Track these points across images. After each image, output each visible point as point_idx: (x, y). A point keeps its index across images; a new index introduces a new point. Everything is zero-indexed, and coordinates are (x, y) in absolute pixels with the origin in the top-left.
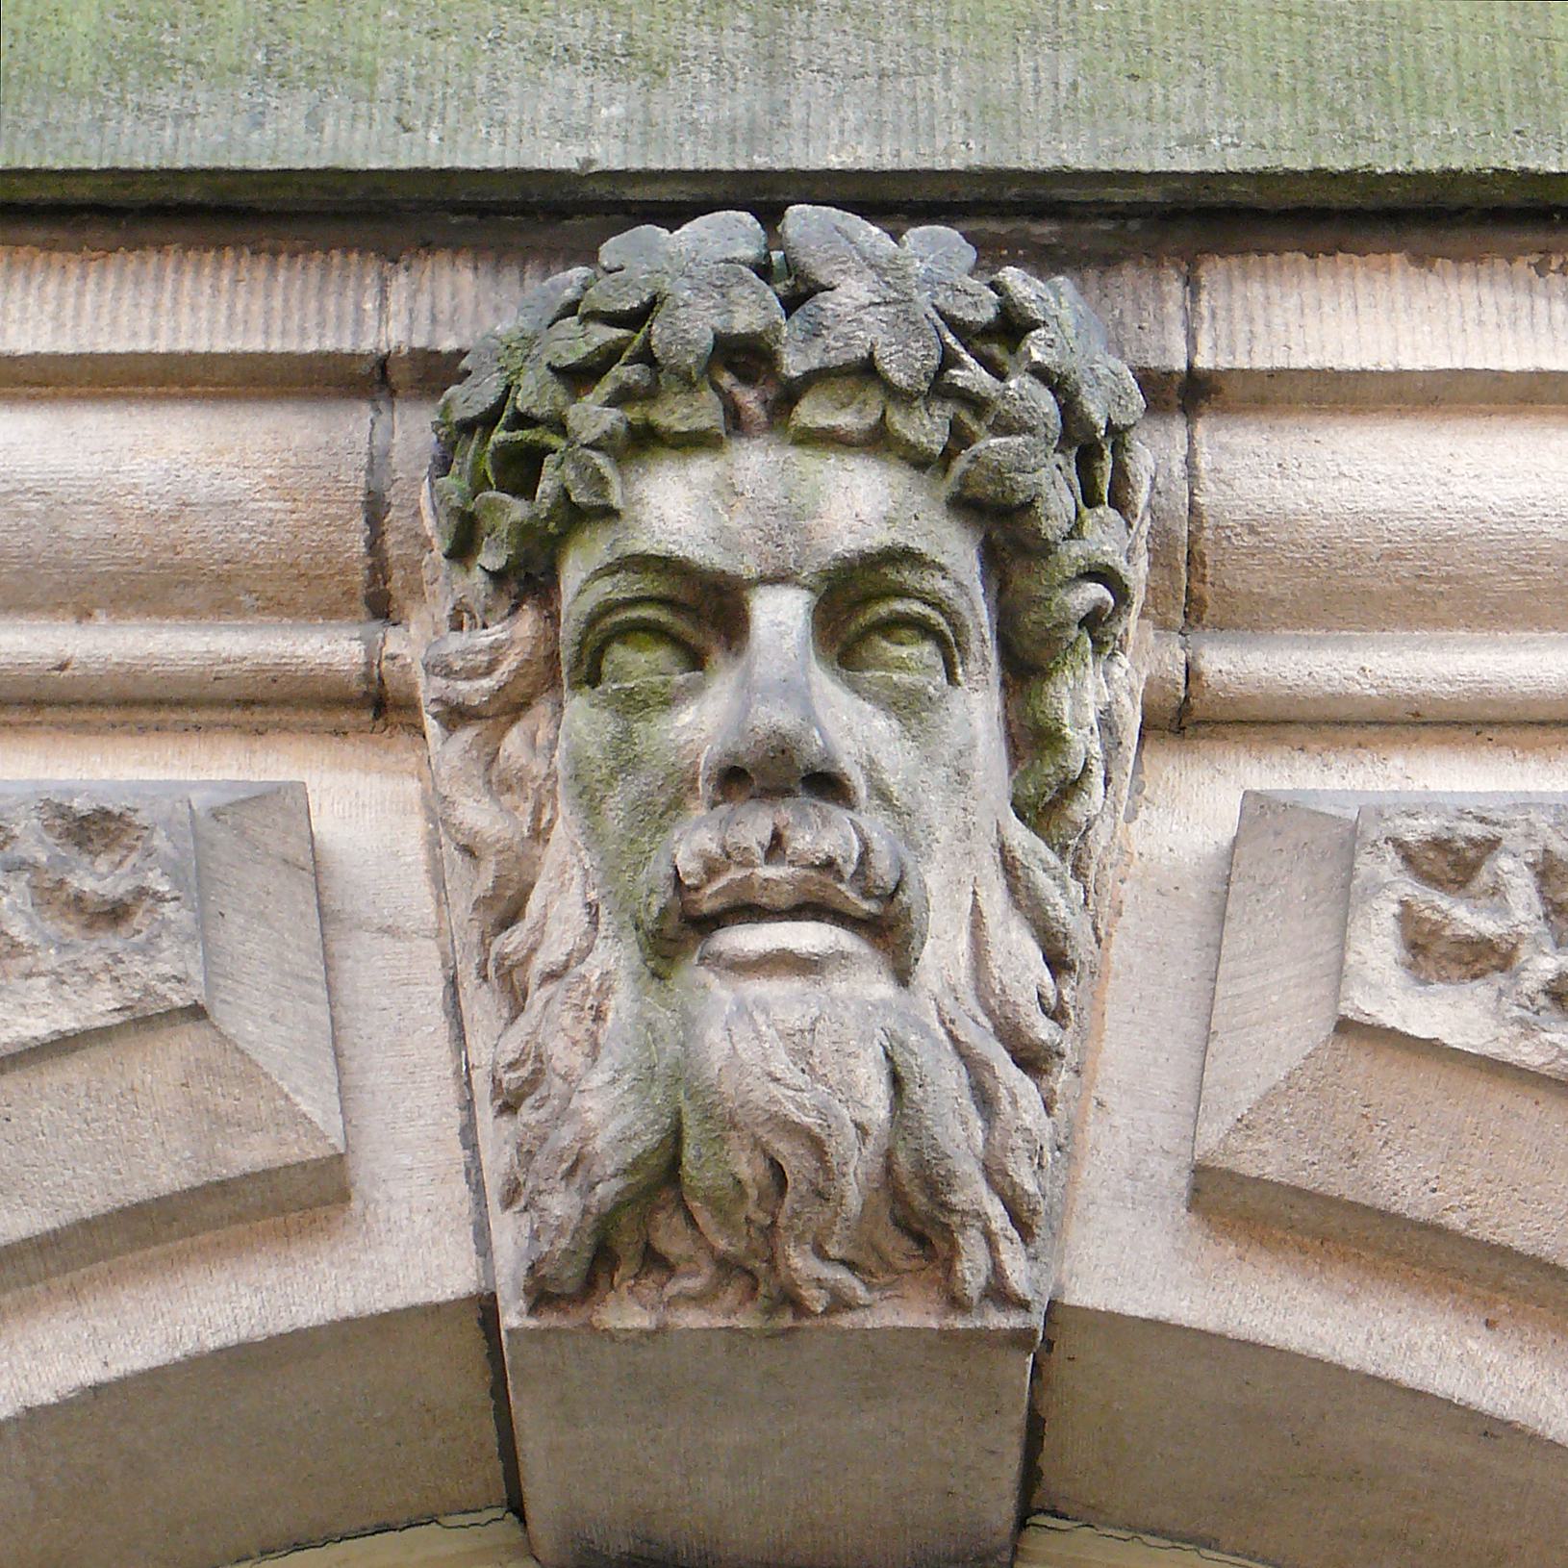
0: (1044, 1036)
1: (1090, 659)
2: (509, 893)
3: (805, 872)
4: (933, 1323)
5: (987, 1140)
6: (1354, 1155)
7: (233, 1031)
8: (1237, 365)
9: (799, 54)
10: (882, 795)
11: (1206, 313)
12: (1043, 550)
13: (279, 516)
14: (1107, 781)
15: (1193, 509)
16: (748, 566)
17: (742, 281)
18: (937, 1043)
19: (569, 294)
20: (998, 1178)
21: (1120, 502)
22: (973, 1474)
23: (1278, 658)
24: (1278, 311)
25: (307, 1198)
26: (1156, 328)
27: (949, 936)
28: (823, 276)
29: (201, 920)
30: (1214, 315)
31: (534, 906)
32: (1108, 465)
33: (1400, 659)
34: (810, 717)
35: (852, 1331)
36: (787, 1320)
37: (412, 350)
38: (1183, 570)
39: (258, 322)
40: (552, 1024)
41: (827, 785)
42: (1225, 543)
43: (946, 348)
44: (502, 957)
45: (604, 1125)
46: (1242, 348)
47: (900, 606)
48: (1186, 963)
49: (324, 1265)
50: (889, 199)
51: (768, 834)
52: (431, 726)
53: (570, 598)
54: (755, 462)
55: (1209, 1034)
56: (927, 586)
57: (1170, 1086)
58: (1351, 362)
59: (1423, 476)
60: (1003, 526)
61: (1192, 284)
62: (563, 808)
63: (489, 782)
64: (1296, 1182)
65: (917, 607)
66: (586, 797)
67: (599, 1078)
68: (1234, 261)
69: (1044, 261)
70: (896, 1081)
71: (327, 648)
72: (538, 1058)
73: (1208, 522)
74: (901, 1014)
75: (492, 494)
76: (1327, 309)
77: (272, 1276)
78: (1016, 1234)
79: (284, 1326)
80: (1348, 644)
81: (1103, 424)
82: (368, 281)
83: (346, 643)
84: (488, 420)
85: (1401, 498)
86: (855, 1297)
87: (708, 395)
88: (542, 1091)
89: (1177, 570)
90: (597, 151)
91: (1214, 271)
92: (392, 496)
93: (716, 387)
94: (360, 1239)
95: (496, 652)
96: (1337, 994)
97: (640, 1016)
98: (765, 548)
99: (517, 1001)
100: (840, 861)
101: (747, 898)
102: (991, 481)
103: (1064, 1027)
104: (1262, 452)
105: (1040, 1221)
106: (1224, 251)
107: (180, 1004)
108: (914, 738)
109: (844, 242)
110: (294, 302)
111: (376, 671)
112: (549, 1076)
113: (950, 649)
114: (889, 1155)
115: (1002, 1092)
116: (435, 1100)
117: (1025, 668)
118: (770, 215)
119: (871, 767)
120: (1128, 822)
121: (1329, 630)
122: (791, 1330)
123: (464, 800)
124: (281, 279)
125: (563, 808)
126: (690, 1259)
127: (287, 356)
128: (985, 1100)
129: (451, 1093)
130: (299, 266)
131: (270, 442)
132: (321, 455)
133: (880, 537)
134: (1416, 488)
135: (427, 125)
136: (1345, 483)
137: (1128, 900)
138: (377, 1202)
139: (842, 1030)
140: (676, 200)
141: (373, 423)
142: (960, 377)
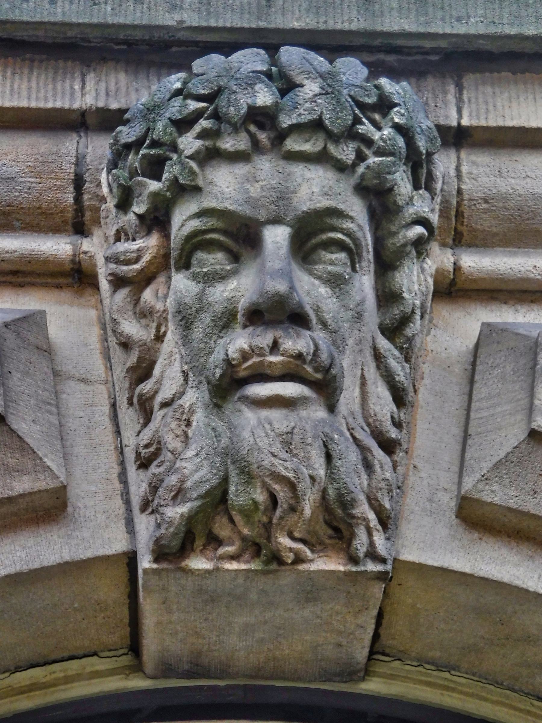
0: (394, 436)
1: (415, 260)
2: (144, 365)
3: (288, 359)
4: (342, 568)
5: (369, 484)
6: (535, 493)
10: (324, 324)
11: (466, 100)
12: (398, 210)
13: (34, 185)
14: (422, 317)
15: (459, 192)
16: (262, 216)
18: (347, 439)
19: (178, 85)
21: (429, 188)
22: (352, 636)
24: (499, 100)
26: (443, 106)
28: (299, 79)
30: (469, 101)
31: (157, 371)
32: (425, 171)
34: (292, 288)
35: (304, 571)
36: (274, 566)
38: (454, 219)
39: (24, 93)
41: (298, 319)
42: (473, 207)
43: (355, 115)
44: (141, 396)
45: (191, 475)
46: (483, 117)
47: (332, 235)
48: (453, 402)
49: (55, 537)
50: (330, 44)
51: (271, 341)
52: (104, 284)
53: (177, 228)
54: (266, 166)
55: (466, 436)
56: (344, 226)
57: (447, 459)
60: (379, 199)
61: (460, 88)
62: (171, 326)
63: (135, 313)
64: (510, 505)
65: (340, 236)
66: (184, 321)
67: (190, 453)
68: (478, 75)
69: (395, 74)
70: (329, 457)
71: (54, 248)
72: (159, 443)
73: (466, 197)
74: (331, 425)
75: (140, 178)
76: (522, 99)
77: (31, 542)
79: (36, 565)
80: (528, 255)
81: (424, 152)
82: (76, 75)
83: (63, 245)
84: (138, 144)
86: (307, 556)
87: (244, 135)
89: (451, 219)
90: (185, 16)
91: (469, 80)
92: (87, 177)
93: (248, 132)
94: (72, 524)
95: (140, 253)
98: (270, 207)
99: (147, 416)
100: (305, 354)
101: (261, 371)
102: (375, 178)
103: (401, 431)
104: (491, 165)
105: (391, 522)
106: (475, 71)
109: (308, 65)
110: (41, 84)
112: (164, 451)
113: (354, 254)
114: (324, 491)
115: (376, 462)
116: (106, 461)
117: (386, 265)
118: (272, 49)
119: (317, 310)
120: (427, 336)
121: (519, 248)
122: (276, 571)
123: (124, 321)
124: (35, 73)
125: (171, 326)
126: (230, 538)
127: (39, 109)
128: (368, 466)
129: (113, 457)
130: (43, 68)
131: (30, 151)
132: (54, 157)
136: (529, 180)
137: (427, 371)
138: (79, 508)
139: (305, 433)
140: (228, 43)
142: (361, 129)
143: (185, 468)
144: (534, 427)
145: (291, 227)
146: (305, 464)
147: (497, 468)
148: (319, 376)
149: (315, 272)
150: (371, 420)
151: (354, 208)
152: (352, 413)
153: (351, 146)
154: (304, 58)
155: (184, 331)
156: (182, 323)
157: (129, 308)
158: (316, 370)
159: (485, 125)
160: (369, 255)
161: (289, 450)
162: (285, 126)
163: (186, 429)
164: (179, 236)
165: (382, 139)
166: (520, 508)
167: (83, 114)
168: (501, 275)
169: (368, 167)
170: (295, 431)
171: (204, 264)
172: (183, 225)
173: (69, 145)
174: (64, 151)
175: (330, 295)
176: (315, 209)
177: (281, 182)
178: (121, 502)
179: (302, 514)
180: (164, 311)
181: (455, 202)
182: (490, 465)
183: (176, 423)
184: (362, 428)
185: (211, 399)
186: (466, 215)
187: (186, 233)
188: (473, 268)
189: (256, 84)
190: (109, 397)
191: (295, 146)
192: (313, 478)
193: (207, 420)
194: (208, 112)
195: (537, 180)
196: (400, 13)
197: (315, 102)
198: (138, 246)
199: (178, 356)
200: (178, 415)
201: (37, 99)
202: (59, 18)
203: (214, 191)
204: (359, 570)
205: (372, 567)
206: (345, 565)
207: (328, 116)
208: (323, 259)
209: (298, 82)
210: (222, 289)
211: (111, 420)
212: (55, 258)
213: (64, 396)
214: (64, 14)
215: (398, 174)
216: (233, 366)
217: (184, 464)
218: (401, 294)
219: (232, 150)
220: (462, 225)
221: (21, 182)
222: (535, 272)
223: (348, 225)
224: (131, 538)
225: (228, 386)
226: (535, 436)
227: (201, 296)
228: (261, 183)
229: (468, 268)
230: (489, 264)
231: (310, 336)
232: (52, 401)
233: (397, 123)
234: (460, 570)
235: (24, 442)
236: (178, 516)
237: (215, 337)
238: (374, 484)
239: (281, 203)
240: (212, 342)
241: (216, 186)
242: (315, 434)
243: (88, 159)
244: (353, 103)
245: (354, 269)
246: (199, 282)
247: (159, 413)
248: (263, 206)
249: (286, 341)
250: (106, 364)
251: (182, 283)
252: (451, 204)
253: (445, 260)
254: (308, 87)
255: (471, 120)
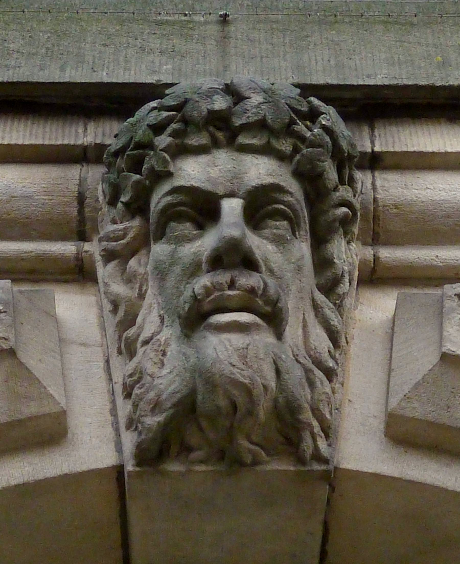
4: (292, 468)
5: (312, 397)
6: (449, 407)
7: (24, 361)
8: (389, 150)
9: (233, 51)
10: (271, 271)
13: (47, 201)
15: (375, 199)
16: (220, 191)
17: (218, 94)
20: (316, 412)
23: (407, 253)
25: (50, 432)
27: (295, 327)
28: (247, 94)
29: (14, 321)
30: (380, 135)
31: (139, 320)
33: (450, 253)
37: (95, 144)
38: (372, 222)
40: (145, 357)
42: (386, 212)
44: (127, 339)
56: (285, 199)
58: (430, 149)
59: (457, 189)
62: (150, 283)
63: (123, 279)
65: (282, 207)
70: (278, 372)
71: (63, 248)
72: (141, 373)
73: (381, 204)
78: (323, 434)
85: (449, 195)
88: (143, 382)
92: (88, 194)
93: (208, 131)
95: (125, 231)
96: (441, 346)
97: (180, 352)
98: (227, 184)
100: (256, 288)
107: (6, 348)
108: (281, 253)
109: (253, 84)
111: (80, 256)
113: (294, 226)
115: (317, 380)
117: (319, 241)
119: (266, 261)
127: (52, 145)
129: (107, 397)
133: (268, 180)
134: (454, 193)
135: (103, 70)
136: (428, 191)
138: (77, 434)
141: (81, 170)
142: (296, 128)
143: (161, 384)
144: (444, 351)
145: (244, 199)
146: (259, 375)
147: (417, 389)
148: (268, 309)
149: (264, 235)
150: (312, 353)
151: (293, 186)
152: (297, 346)
153: (289, 140)
154: (251, 80)
155: (160, 283)
156: (159, 276)
157: (118, 275)
158: (267, 303)
159: (392, 150)
160: (306, 226)
161: (245, 363)
162: (237, 125)
163: (162, 358)
164: (156, 212)
165: (312, 134)
166: (437, 421)
167: (85, 148)
168: (411, 263)
169: (303, 155)
170: (249, 347)
171: (176, 230)
172: (158, 203)
173: (74, 173)
174: (71, 176)
175: (276, 251)
176: (262, 185)
177: (235, 166)
178: (112, 429)
179: (258, 418)
180: (145, 273)
181: (372, 208)
182: (411, 387)
183: (154, 353)
184: (305, 357)
185: (182, 331)
186: (381, 218)
187: (161, 208)
188: (389, 258)
189: (213, 95)
190: (104, 355)
191: (245, 141)
192: (265, 387)
193: (179, 348)
194: (178, 118)
195: (435, 190)
196: (324, 73)
197: (260, 107)
198: (124, 226)
199: (155, 305)
200: (155, 347)
201: (50, 139)
202: (67, 80)
203: (182, 174)
204: (306, 469)
205: (317, 467)
206: (294, 466)
207: (270, 117)
208: (269, 225)
209: (246, 96)
210: (190, 246)
211: (105, 371)
212: (63, 256)
213: (68, 355)
214: (70, 77)
215: (326, 163)
216: (199, 301)
217: (160, 381)
218: (332, 260)
219: (196, 144)
220: (379, 226)
221: (37, 199)
222: (437, 260)
223: (288, 198)
224: (119, 455)
225: (195, 319)
226: (446, 358)
227: (173, 254)
228: (218, 167)
229: (385, 258)
230: (401, 255)
231: (260, 276)
232: (56, 350)
233: (324, 125)
234: (390, 475)
235: (32, 373)
236: (156, 424)
237: (184, 283)
238: (316, 397)
239: (235, 181)
240: (182, 287)
241: (184, 170)
242: (266, 352)
243: (89, 181)
244: (289, 109)
245: (294, 234)
246: (172, 244)
247: (141, 349)
248: (222, 183)
249: (241, 279)
250: (102, 333)
251: (160, 249)
252: (369, 210)
253: (367, 253)
254: (254, 98)
255: (381, 147)
